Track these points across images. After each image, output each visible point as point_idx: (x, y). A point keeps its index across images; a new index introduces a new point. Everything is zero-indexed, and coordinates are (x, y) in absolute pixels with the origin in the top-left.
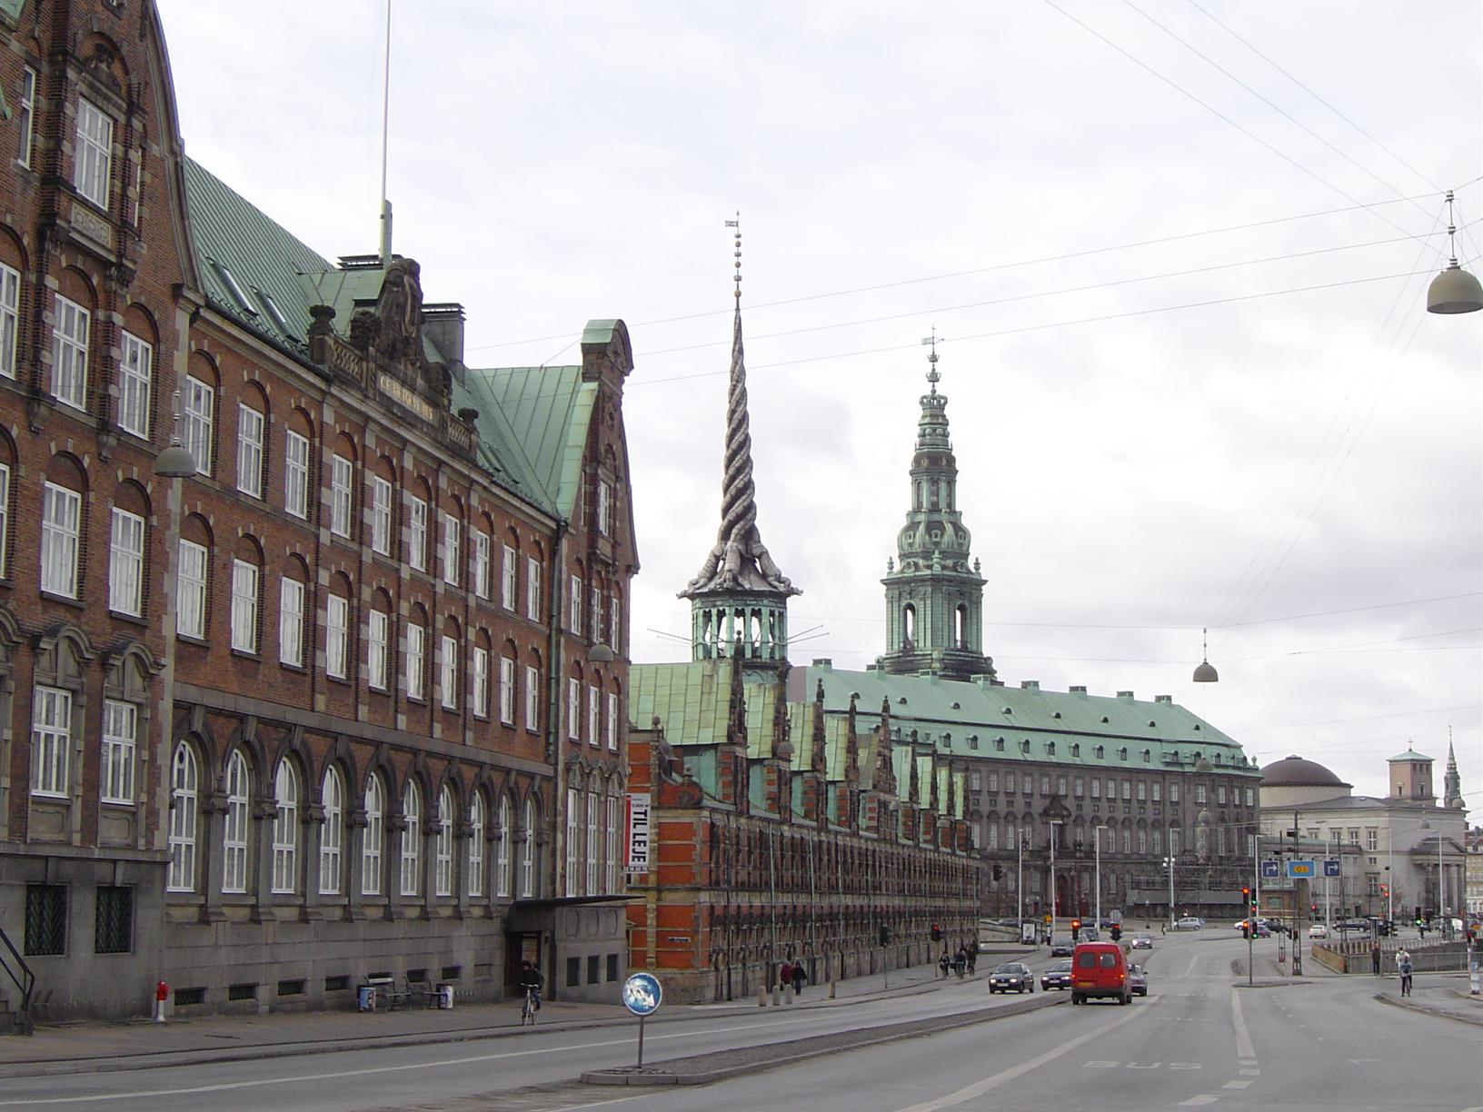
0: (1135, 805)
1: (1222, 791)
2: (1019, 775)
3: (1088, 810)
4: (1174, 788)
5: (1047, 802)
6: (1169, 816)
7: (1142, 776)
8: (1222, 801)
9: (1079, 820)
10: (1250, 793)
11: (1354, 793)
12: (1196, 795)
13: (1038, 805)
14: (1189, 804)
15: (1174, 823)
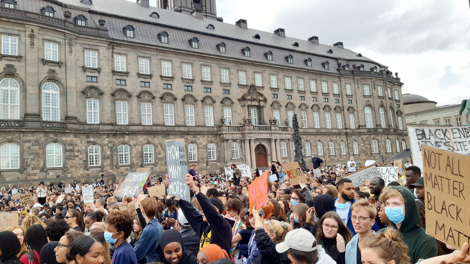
0: (320, 97)
1: (380, 88)
2: (216, 68)
3: (283, 98)
4: (348, 87)
5: (245, 91)
6: (346, 104)
7: (324, 78)
8: (380, 94)
9: (275, 105)
10: (396, 93)
11: (437, 105)
12: (363, 91)
13: (236, 93)
14: (359, 96)
15: (351, 109)
